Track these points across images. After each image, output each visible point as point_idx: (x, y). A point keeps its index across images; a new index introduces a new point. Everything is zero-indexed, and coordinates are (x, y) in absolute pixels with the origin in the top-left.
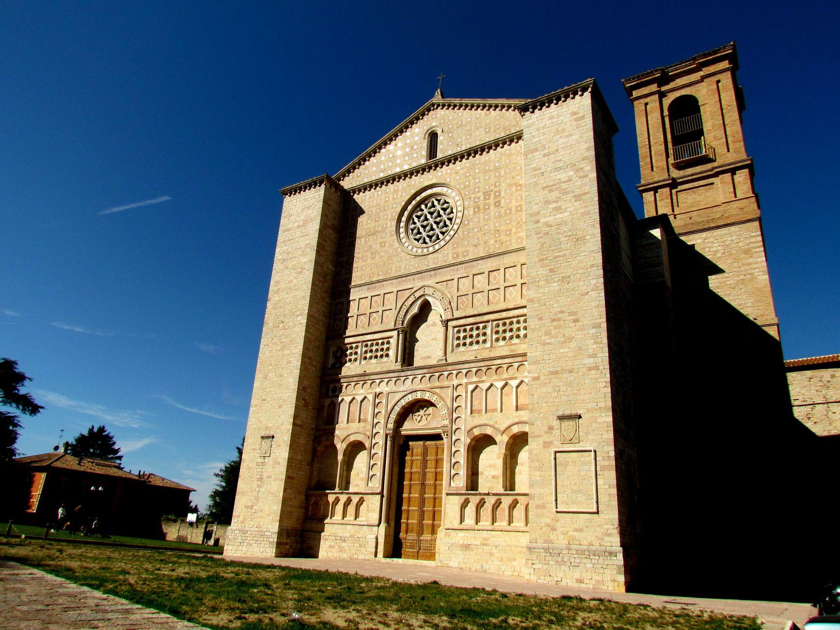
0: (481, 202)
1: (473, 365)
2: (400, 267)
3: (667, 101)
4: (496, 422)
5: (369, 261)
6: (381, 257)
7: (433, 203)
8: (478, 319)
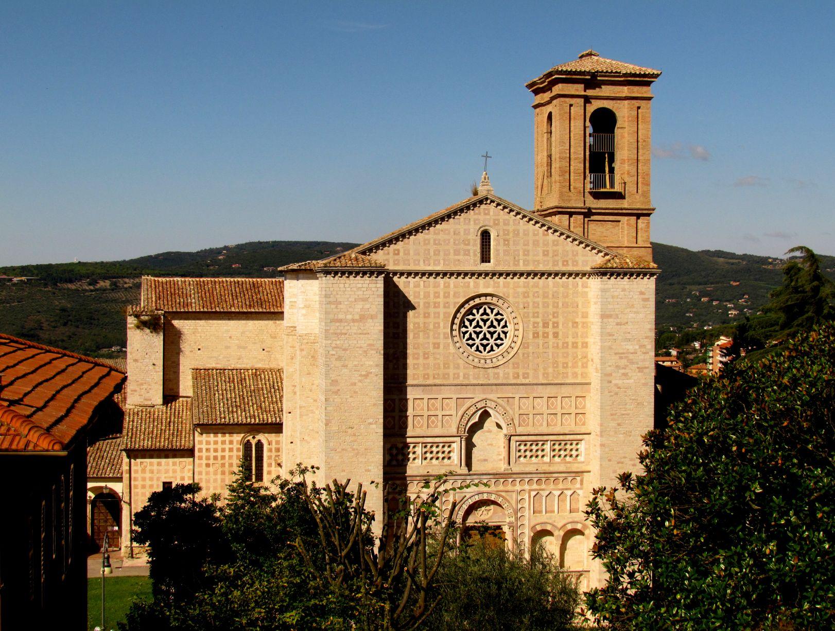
0: (541, 330)
3: (591, 109)
7: (485, 309)
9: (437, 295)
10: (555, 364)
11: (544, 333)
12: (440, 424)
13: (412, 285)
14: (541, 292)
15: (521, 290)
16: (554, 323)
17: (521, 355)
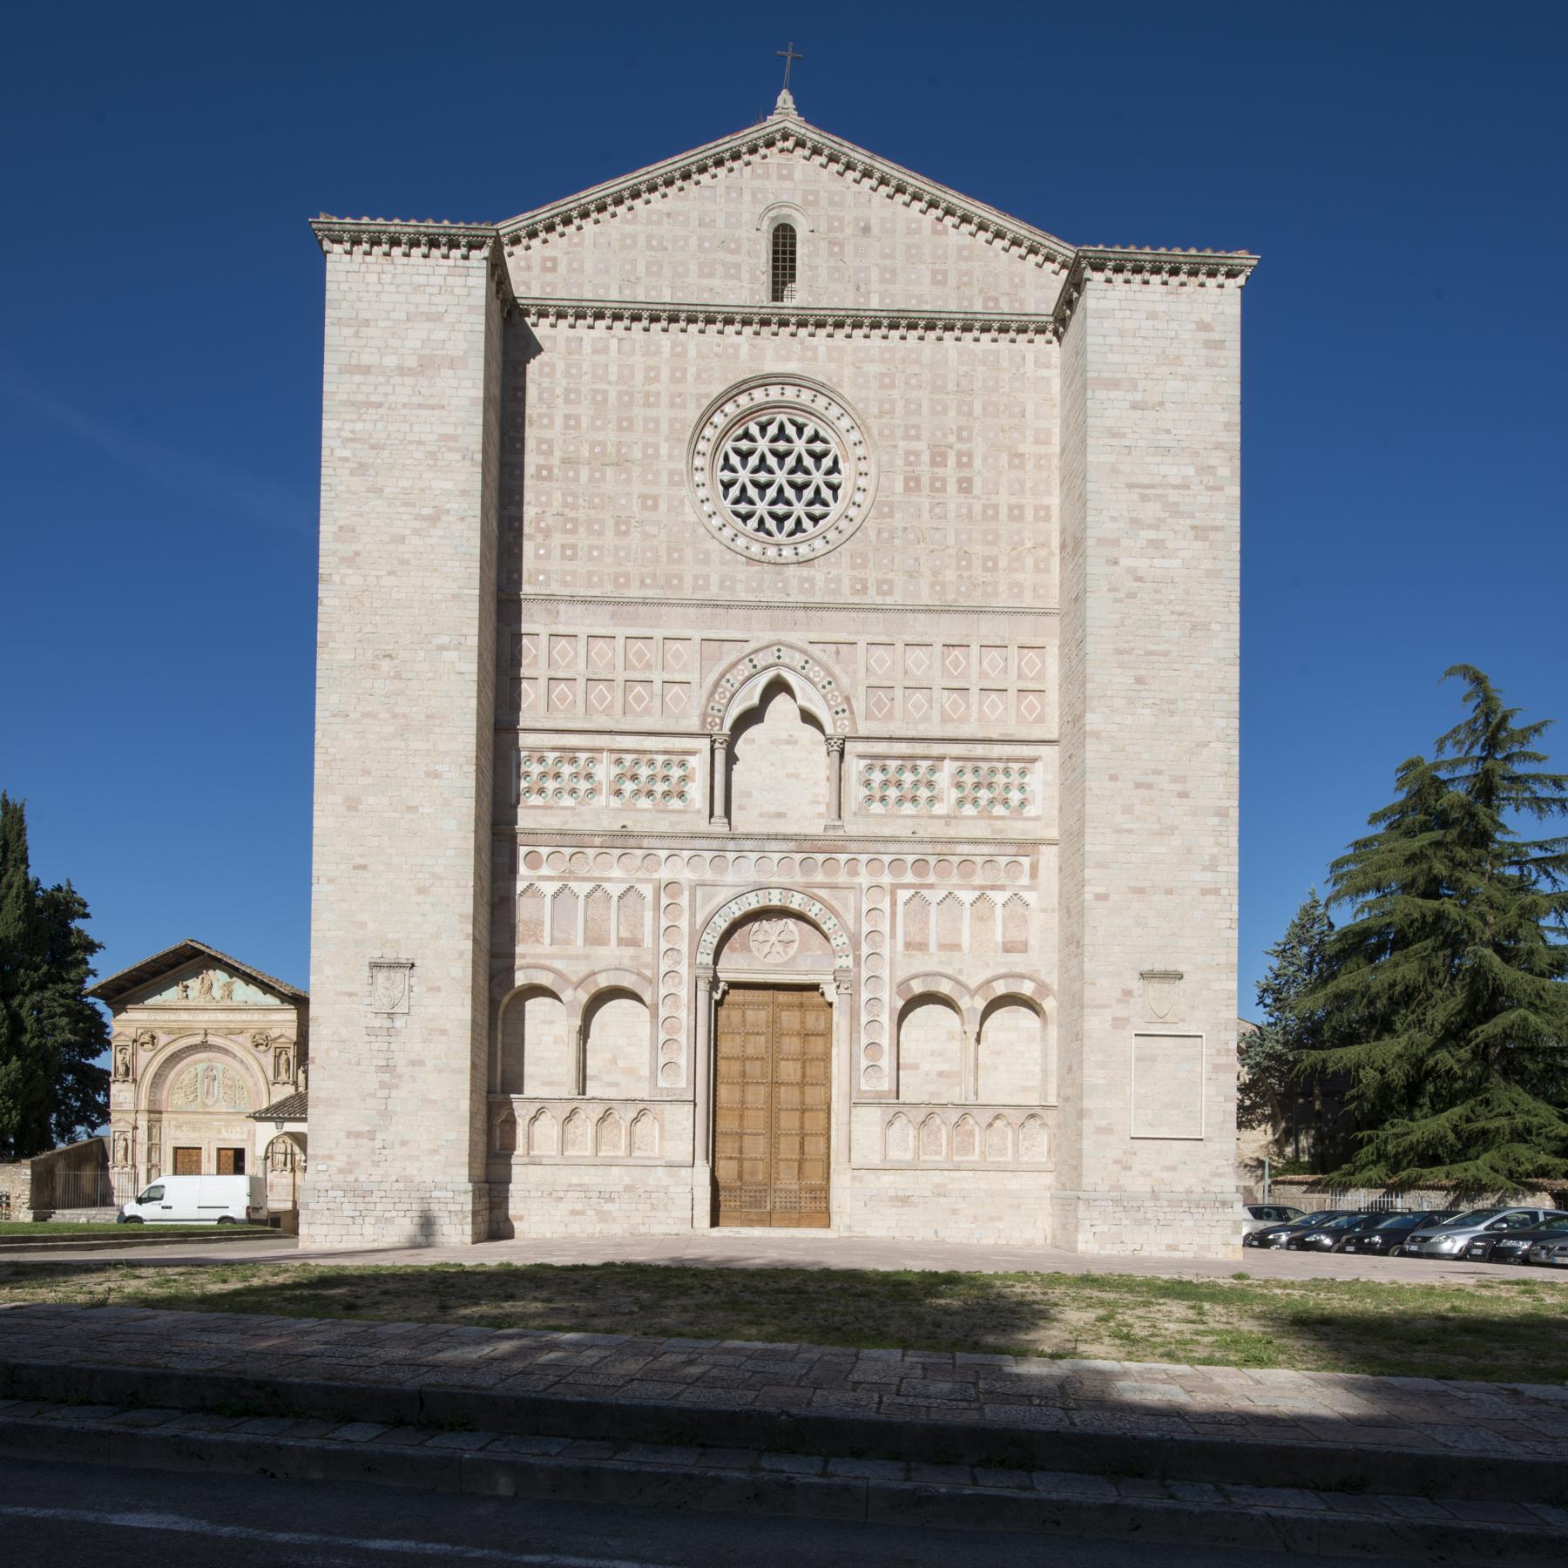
0: (925, 471)
1: (906, 847)
2: (707, 578)
4: (960, 971)
8: (919, 749)
9: (652, 375)
11: (933, 479)
12: (657, 703)
13: (587, 348)
16: (959, 455)
17: (872, 534)
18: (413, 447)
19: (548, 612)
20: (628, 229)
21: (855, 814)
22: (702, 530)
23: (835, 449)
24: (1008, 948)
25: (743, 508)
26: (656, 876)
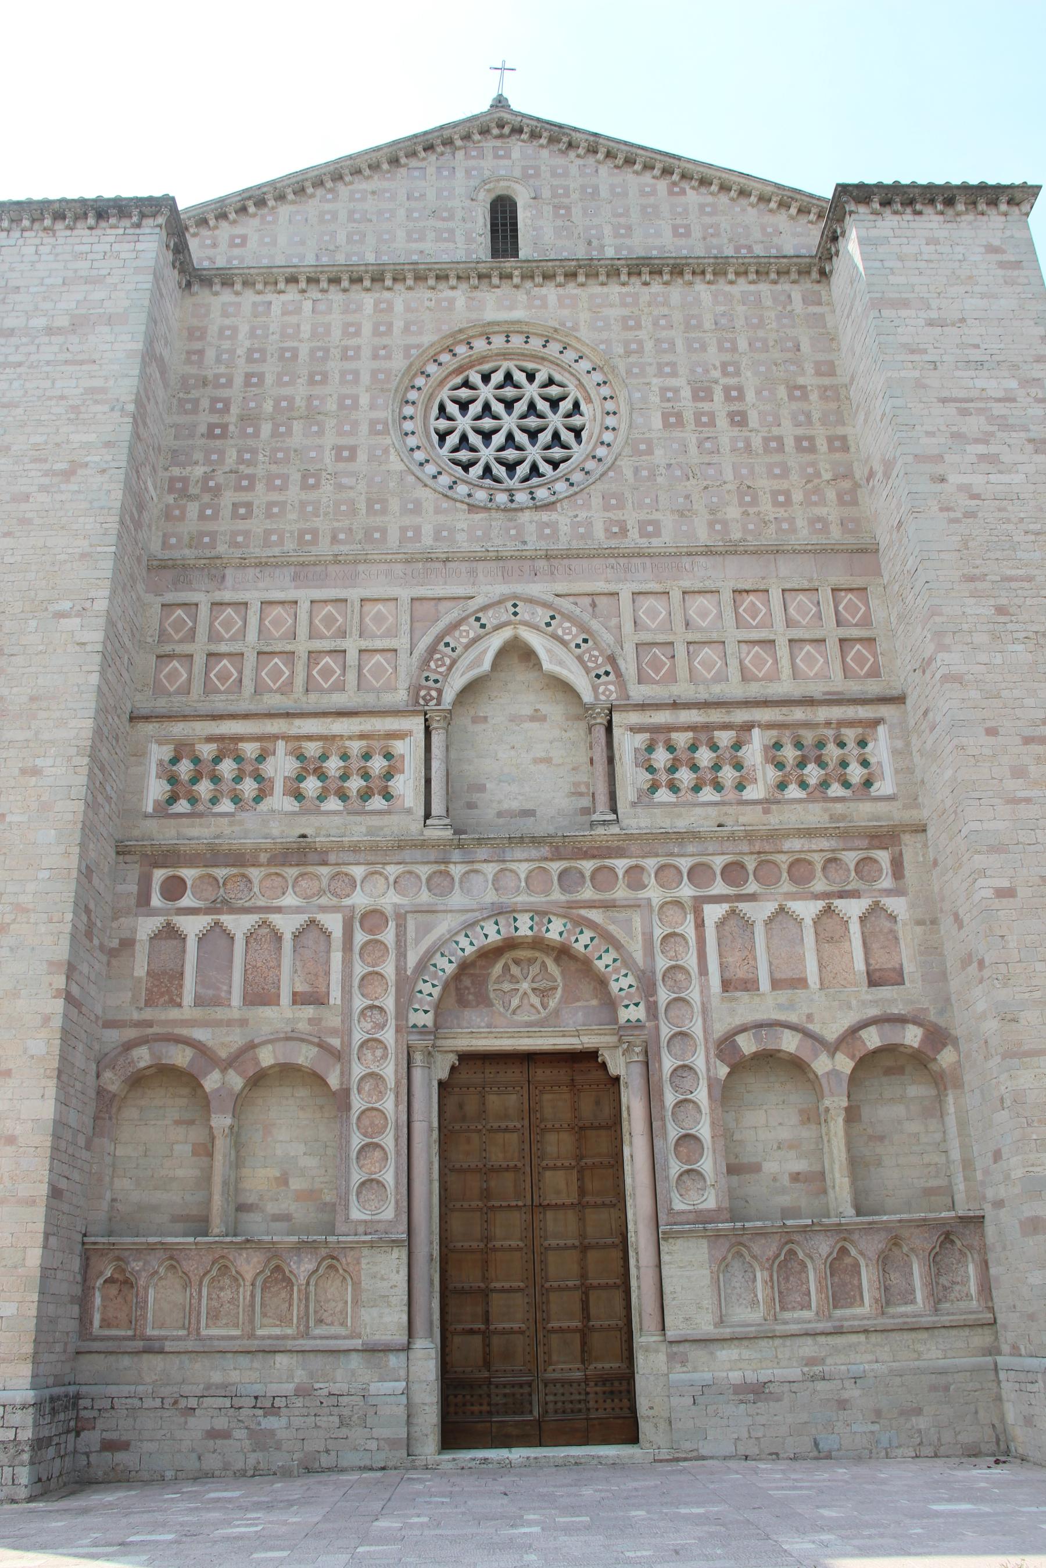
2: (417, 530)
4: (810, 1017)
5: (294, 493)
6: (340, 487)
8: (716, 716)
9: (352, 330)
10: (747, 492)
11: (698, 415)
12: (351, 677)
13: (276, 310)
14: (677, 317)
15: (614, 313)
16: (727, 390)
18: (53, 403)
19: (212, 578)
20: (327, 206)
21: (634, 804)
22: (411, 479)
23: (574, 392)
24: (874, 980)
25: (464, 455)
26: (347, 902)
